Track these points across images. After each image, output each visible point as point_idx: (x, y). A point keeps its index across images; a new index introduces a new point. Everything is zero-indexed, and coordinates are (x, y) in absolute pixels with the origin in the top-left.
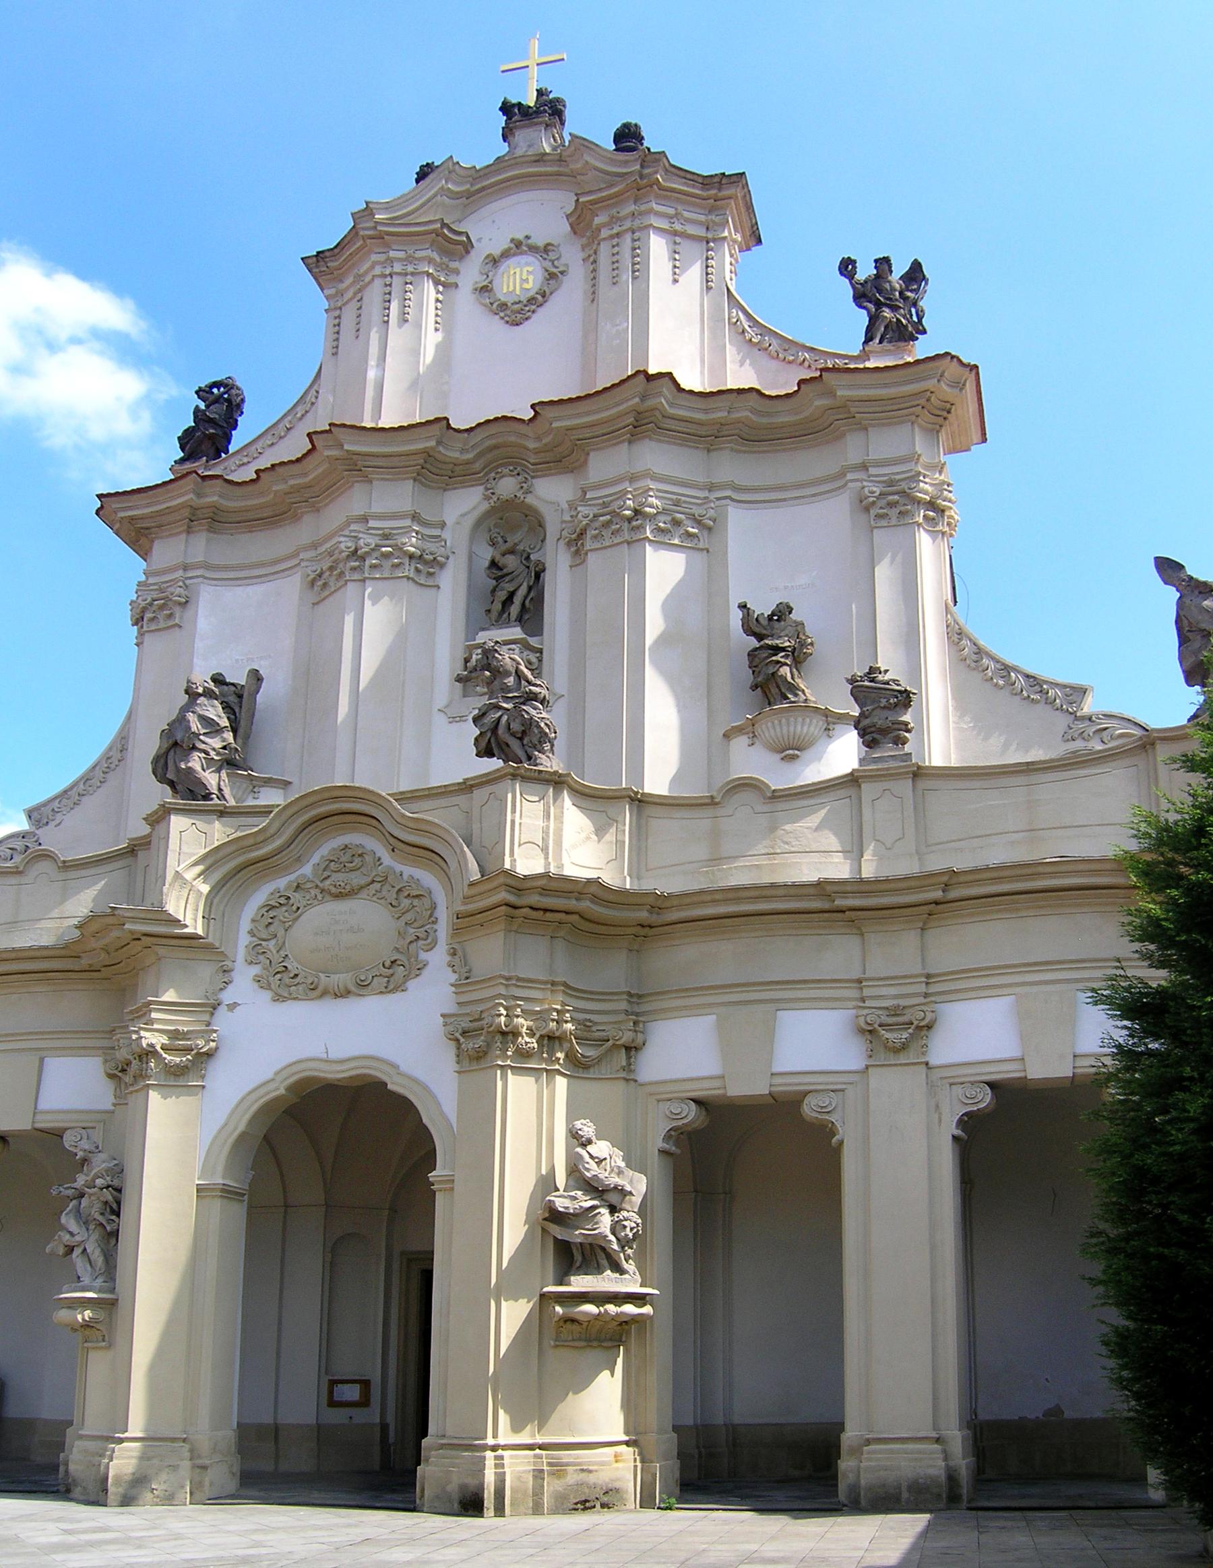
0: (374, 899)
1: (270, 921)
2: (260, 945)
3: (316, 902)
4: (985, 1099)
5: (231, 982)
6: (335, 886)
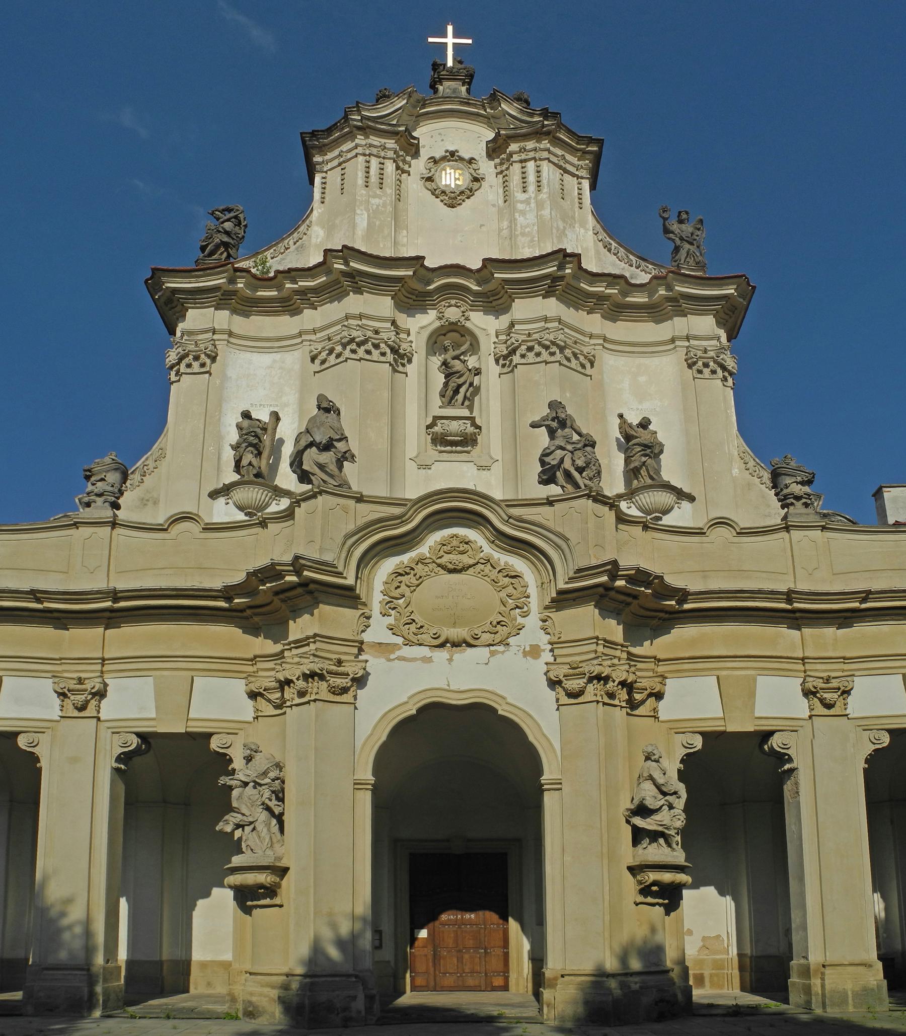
0: (479, 575)
1: (399, 584)
2: (392, 602)
3: (433, 574)
4: (886, 740)
5: (369, 626)
6: (451, 563)
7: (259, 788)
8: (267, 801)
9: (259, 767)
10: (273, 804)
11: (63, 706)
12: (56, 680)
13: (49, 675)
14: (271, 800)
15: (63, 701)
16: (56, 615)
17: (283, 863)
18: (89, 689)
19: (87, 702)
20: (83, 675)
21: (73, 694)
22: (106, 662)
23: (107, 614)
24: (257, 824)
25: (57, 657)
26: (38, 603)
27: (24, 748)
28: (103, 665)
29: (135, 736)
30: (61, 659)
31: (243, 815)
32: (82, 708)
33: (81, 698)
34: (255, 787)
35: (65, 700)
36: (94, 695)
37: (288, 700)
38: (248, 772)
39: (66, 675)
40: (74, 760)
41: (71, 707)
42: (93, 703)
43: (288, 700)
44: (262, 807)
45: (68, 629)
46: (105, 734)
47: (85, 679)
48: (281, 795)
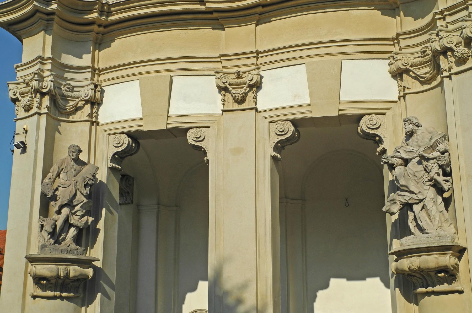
7: (425, 163)
8: (436, 177)
9: (421, 142)
10: (441, 179)
11: (224, 101)
12: (219, 75)
13: (212, 72)
14: (439, 175)
15: (224, 95)
16: (215, 15)
17: (462, 243)
18: (248, 82)
19: (246, 94)
20: (242, 69)
21: (233, 88)
22: (260, 55)
23: (260, 9)
24: (426, 202)
25: (218, 55)
26: (200, 5)
27: (193, 143)
28: (257, 59)
29: (291, 124)
30: (220, 56)
31: (412, 192)
32: (240, 102)
33: (240, 92)
34: (419, 163)
35: (226, 94)
36: (251, 87)
37: (445, 70)
38: (409, 148)
39: (225, 70)
40: (237, 151)
41: (231, 99)
42: (251, 95)
43: (445, 70)
44: (429, 183)
45: (224, 29)
46: (264, 124)
47: (243, 73)
48: (448, 169)
